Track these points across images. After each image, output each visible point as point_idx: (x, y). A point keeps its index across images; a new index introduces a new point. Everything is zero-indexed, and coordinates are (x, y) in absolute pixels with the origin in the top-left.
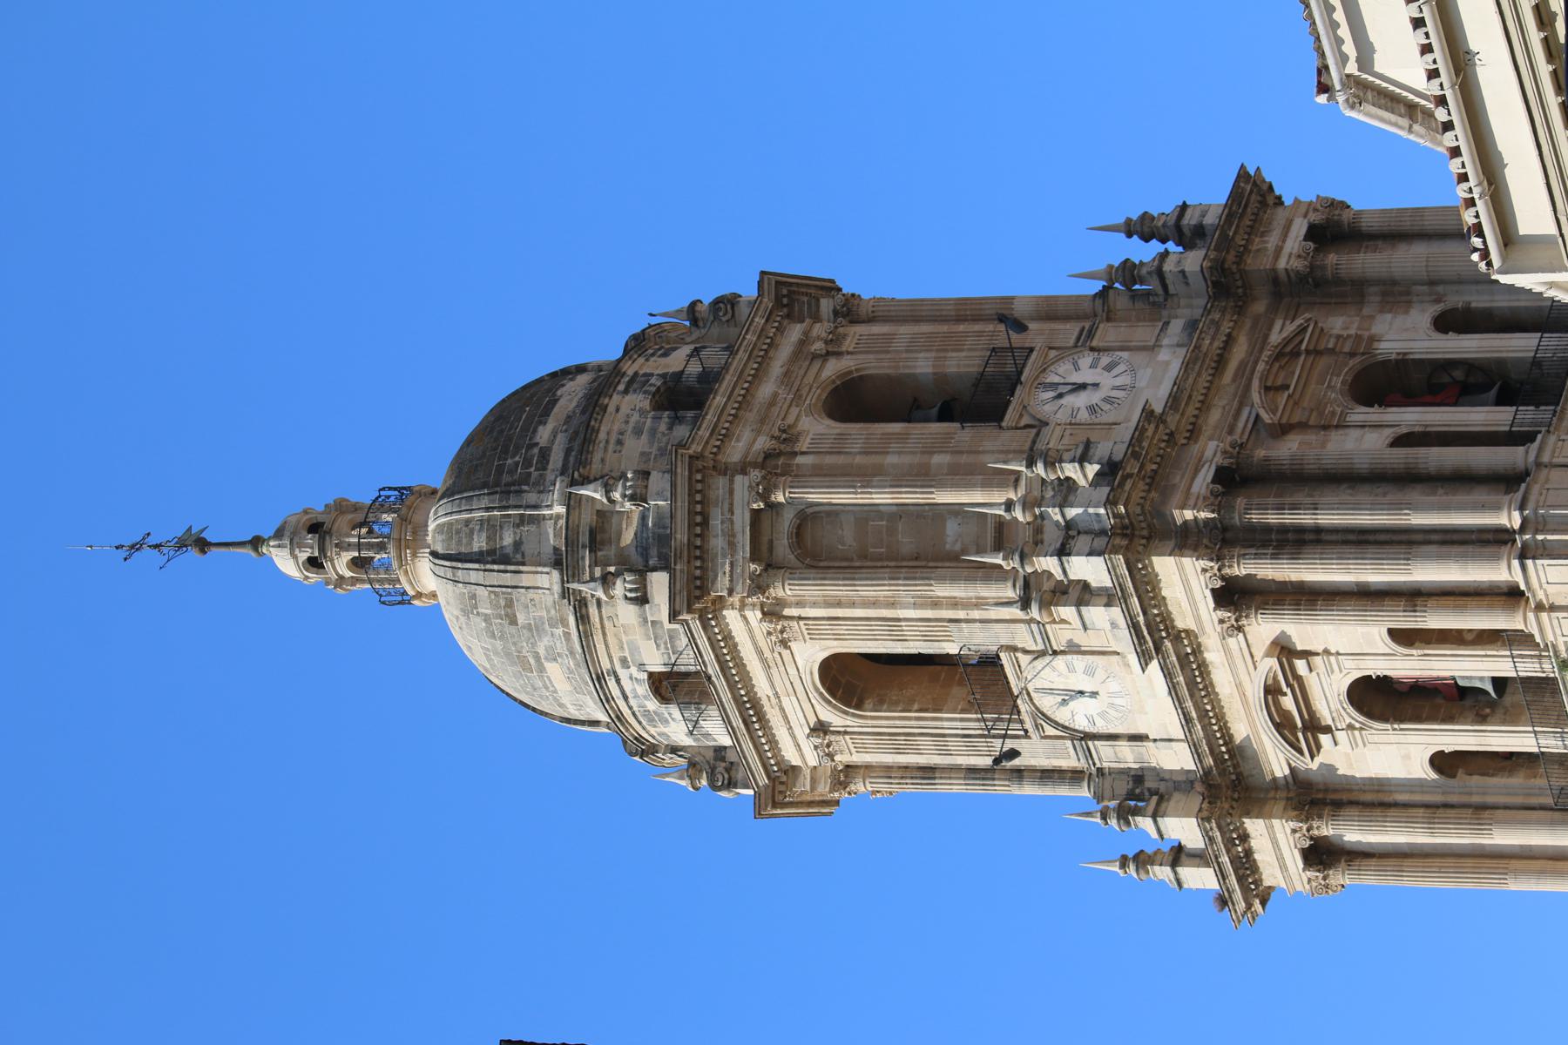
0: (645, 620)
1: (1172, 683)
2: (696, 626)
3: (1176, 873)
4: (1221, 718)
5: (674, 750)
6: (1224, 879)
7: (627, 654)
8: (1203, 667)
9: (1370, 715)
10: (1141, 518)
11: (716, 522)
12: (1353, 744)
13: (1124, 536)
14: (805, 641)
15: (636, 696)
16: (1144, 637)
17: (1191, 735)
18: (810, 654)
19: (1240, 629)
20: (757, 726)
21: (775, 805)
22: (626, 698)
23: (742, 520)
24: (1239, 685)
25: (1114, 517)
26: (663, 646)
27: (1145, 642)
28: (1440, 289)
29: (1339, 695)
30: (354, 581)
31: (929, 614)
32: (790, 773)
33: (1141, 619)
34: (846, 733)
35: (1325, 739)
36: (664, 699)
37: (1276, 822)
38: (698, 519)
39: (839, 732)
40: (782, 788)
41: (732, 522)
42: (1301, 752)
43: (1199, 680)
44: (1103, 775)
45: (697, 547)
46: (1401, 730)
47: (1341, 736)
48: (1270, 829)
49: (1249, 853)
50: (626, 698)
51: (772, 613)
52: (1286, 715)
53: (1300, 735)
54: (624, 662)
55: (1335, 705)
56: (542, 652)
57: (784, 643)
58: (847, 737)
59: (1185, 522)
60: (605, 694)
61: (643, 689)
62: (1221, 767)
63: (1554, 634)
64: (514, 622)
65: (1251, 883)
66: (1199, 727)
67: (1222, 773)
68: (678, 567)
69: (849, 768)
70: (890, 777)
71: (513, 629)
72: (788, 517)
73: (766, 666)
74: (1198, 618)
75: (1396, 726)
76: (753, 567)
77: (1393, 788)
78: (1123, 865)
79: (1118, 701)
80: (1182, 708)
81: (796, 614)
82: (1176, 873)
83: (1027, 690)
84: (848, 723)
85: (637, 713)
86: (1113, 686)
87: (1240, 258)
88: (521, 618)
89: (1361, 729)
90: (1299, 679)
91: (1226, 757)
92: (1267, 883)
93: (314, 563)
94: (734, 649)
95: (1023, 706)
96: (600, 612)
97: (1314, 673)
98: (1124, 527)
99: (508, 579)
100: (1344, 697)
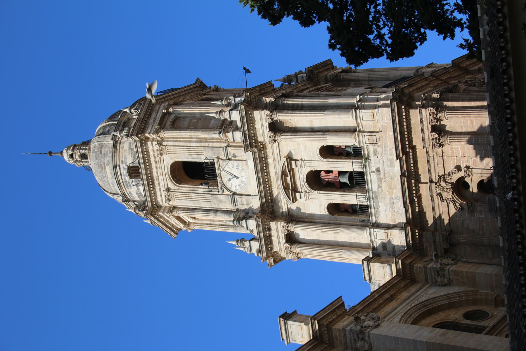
0: (130, 149)
1: (256, 166)
2: (138, 143)
3: (250, 244)
4: (270, 186)
5: (134, 201)
6: (261, 242)
7: (123, 159)
8: (267, 164)
9: (312, 188)
10: (254, 100)
11: (153, 116)
12: (306, 199)
13: (247, 103)
14: (167, 155)
15: (124, 175)
16: (247, 140)
17: (260, 188)
18: (169, 160)
19: (275, 141)
20: (151, 186)
21: (152, 215)
22: (121, 175)
23: (160, 115)
24: (276, 172)
25: (246, 96)
26: (132, 156)
27: (247, 142)
28: (371, 82)
29: (303, 178)
30: (80, 161)
31: (198, 144)
32: (159, 207)
33: (247, 132)
34: (174, 192)
35: (298, 195)
36: (131, 177)
37: (279, 223)
38: (148, 113)
39: (172, 191)
40: (155, 211)
41: (157, 115)
42: (290, 200)
43: (265, 168)
44: (238, 211)
45: (145, 120)
46: (320, 193)
47: (302, 194)
48: (277, 225)
49: (270, 236)
50: (121, 175)
51: (160, 143)
52: (287, 184)
53: (290, 191)
54: (122, 161)
55: (302, 183)
56: (106, 162)
57: (161, 154)
58: (174, 193)
59: (266, 103)
60: (116, 173)
61: (125, 172)
62: (268, 204)
63: (363, 142)
64: (101, 153)
65: (270, 247)
66: (262, 186)
67: (268, 207)
68: (138, 123)
69: (174, 207)
70: (184, 211)
71: (100, 155)
72: (172, 117)
73: (156, 164)
74: (264, 136)
75: (318, 192)
76: (157, 126)
77: (315, 218)
78: (237, 241)
79: (244, 180)
80: (258, 177)
81: (166, 145)
82: (250, 244)
83: (221, 175)
84: (175, 188)
85: (124, 182)
86: (243, 174)
87: (319, 72)
88: (103, 152)
89: (309, 192)
90: (293, 169)
91: (270, 201)
92: (275, 250)
93: (72, 156)
94: (149, 156)
95: (219, 181)
96: (120, 145)
97: (297, 168)
98: (248, 101)
99: (103, 139)
100: (305, 179)
